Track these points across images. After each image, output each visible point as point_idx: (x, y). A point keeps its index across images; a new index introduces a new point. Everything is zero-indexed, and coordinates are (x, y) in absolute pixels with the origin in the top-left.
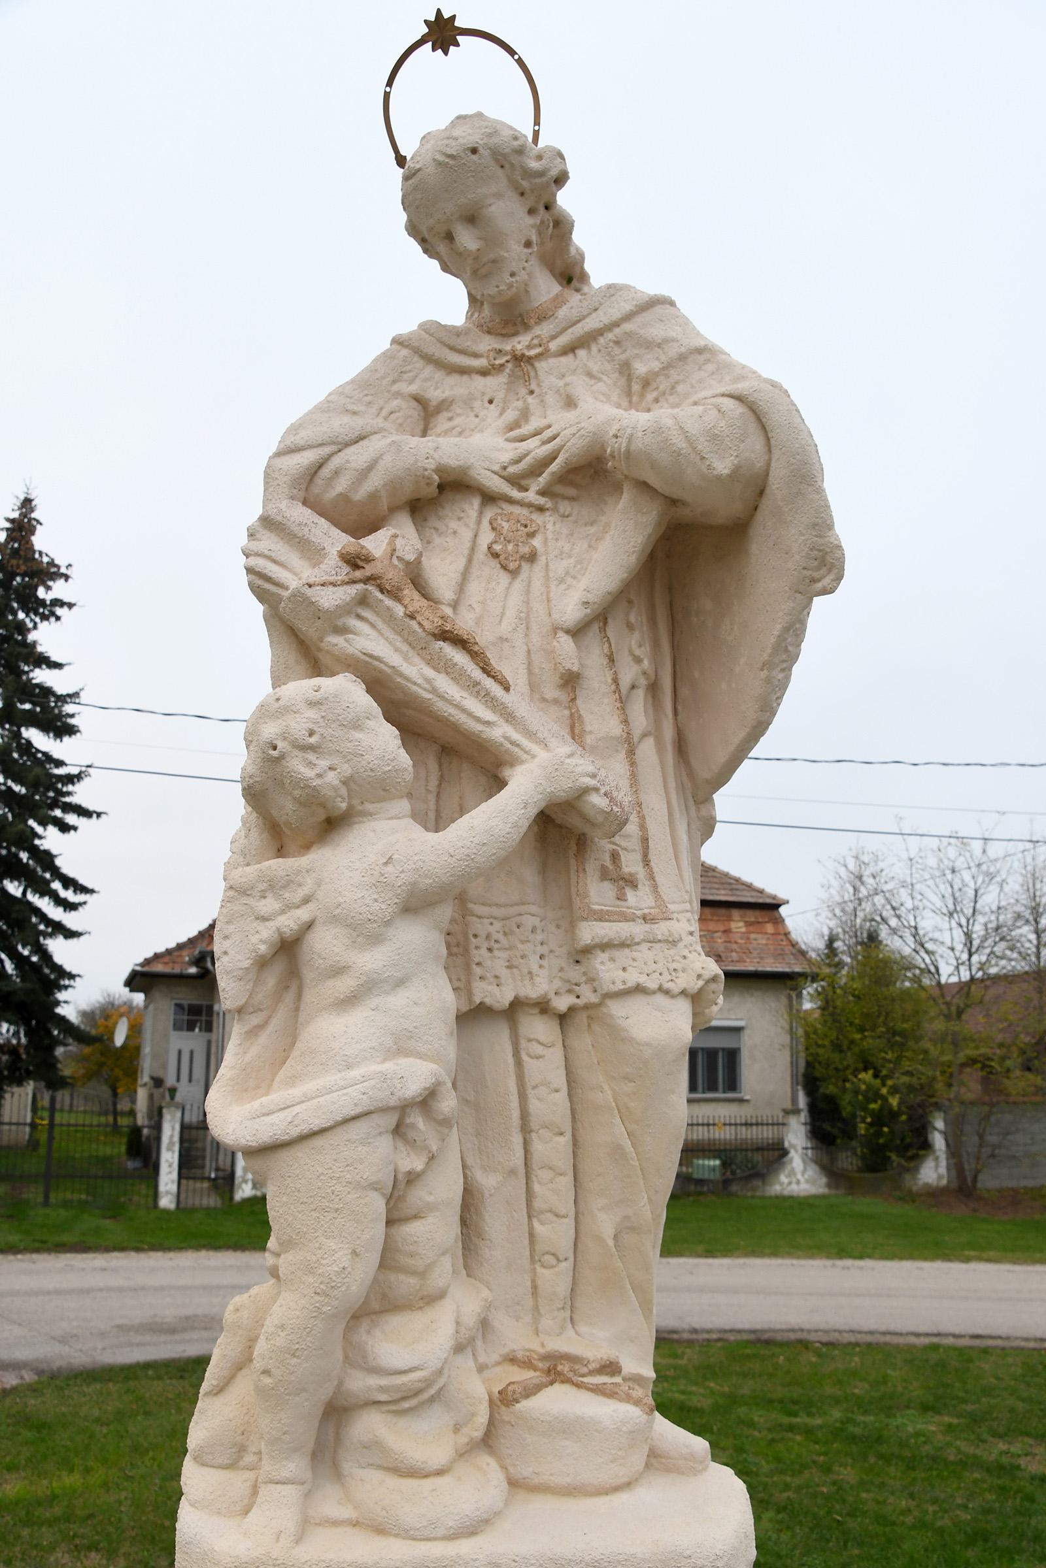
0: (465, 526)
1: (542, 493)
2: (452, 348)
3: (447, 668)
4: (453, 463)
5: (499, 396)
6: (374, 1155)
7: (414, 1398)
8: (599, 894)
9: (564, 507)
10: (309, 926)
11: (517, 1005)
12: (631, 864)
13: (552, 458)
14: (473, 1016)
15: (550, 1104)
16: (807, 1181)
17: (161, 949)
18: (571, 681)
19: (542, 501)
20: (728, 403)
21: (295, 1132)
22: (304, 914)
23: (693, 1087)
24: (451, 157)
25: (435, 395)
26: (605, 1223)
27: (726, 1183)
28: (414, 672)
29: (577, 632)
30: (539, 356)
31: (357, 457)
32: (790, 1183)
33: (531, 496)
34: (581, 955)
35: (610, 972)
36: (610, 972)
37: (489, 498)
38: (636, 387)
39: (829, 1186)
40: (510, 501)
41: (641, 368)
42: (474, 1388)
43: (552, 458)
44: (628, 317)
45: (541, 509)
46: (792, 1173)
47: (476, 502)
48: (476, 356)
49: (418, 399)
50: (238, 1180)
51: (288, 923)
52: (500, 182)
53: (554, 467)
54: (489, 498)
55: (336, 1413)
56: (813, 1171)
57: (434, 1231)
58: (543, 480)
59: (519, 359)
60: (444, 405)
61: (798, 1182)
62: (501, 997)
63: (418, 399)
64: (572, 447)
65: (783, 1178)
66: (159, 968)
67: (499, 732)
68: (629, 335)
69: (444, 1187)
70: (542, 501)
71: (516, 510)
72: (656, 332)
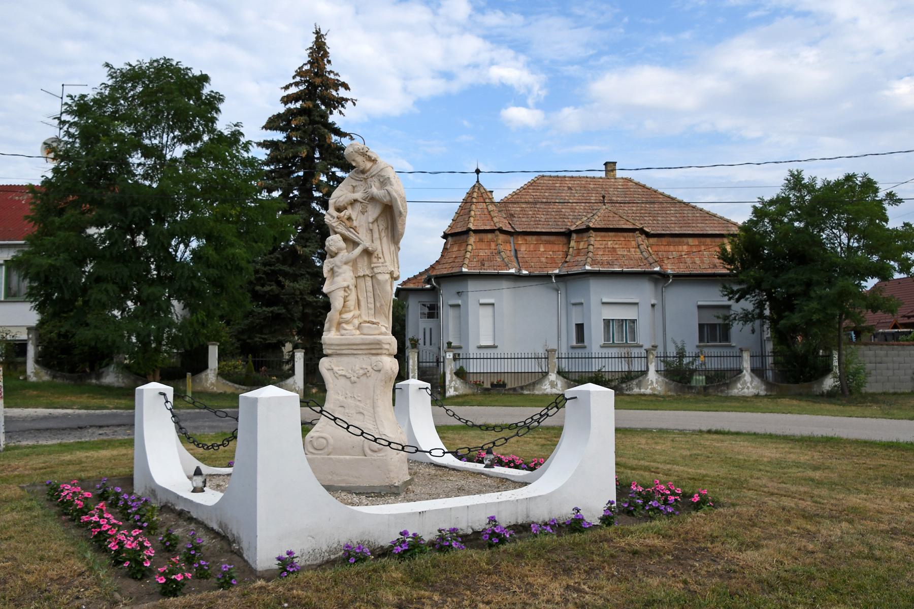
0: (358, 207)
6: (342, 293)
7: (347, 322)
8: (375, 260)
11: (364, 276)
12: (380, 255)
14: (357, 278)
15: (370, 289)
16: (753, 388)
17: (411, 276)
18: (371, 230)
23: (701, 339)
26: (378, 305)
27: (705, 388)
28: (347, 233)
29: (372, 223)
31: (341, 199)
32: (743, 389)
34: (373, 268)
35: (376, 270)
36: (376, 270)
39: (766, 390)
42: (356, 322)
46: (745, 383)
50: (447, 387)
52: (356, 155)
55: (339, 324)
56: (757, 381)
57: (352, 302)
61: (748, 388)
62: (362, 274)
65: (739, 386)
66: (411, 286)
67: (357, 240)
69: (352, 298)
72: (383, 174)
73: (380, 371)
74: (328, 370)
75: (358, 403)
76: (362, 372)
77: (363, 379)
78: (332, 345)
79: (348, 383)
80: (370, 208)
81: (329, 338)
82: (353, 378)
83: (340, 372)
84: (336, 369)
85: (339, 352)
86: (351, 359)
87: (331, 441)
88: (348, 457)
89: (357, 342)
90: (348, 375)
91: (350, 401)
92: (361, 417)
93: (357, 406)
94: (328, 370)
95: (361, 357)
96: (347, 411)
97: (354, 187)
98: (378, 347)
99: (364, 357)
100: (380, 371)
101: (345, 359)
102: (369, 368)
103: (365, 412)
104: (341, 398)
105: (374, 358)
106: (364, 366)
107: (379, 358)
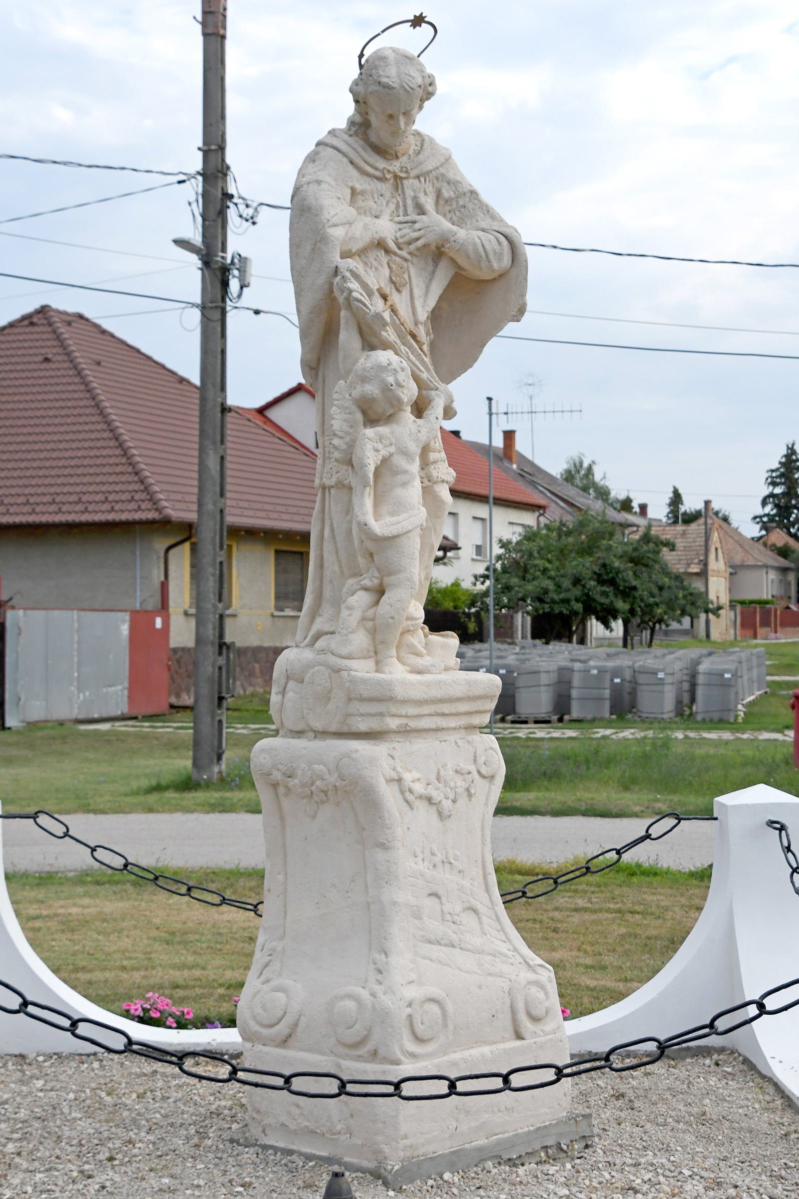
1: (410, 253)
2: (365, 162)
3: (410, 347)
4: (383, 236)
5: (388, 194)
9: (415, 260)
10: (391, 455)
13: (417, 239)
19: (408, 257)
20: (502, 239)
21: (404, 531)
22: (392, 449)
24: (412, 89)
25: (358, 187)
30: (407, 178)
33: (404, 253)
37: (387, 251)
38: (442, 202)
40: (395, 254)
41: (447, 193)
43: (417, 239)
44: (442, 165)
45: (406, 260)
47: (383, 252)
48: (376, 169)
49: (353, 190)
51: (384, 452)
53: (419, 243)
54: (387, 251)
58: (412, 247)
59: (396, 177)
60: (363, 193)
63: (353, 190)
64: (431, 238)
68: (443, 175)
70: (408, 257)
71: (398, 259)
74: (389, 781)
78: (404, 702)
80: (416, 276)
94: (389, 781)
97: (354, 192)
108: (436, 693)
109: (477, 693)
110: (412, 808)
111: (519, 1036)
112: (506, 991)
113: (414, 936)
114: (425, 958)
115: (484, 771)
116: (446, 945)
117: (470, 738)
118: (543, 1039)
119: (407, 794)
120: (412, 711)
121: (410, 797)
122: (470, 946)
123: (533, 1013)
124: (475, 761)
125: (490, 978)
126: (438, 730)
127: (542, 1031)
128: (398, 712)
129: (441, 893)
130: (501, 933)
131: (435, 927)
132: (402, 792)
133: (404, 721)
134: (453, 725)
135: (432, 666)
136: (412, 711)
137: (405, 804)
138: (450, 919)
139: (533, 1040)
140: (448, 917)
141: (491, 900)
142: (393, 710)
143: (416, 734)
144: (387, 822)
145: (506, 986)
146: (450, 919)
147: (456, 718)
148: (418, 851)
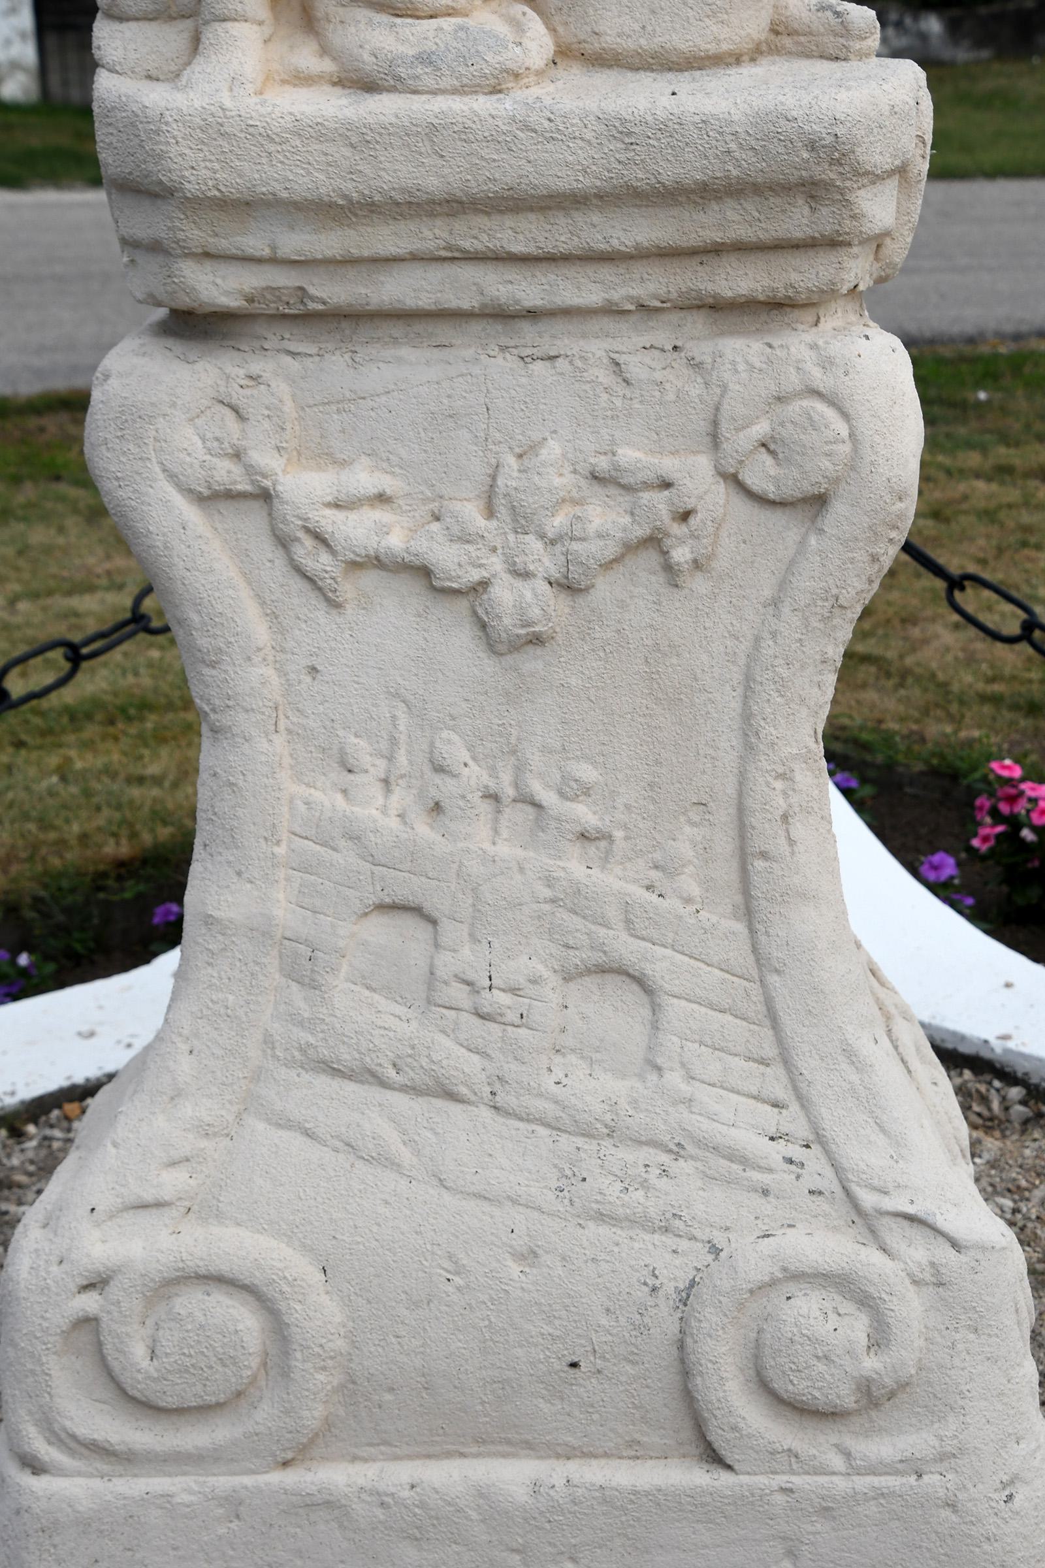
73: (816, 503)
74: (213, 498)
75: (575, 866)
76: (606, 519)
77: (630, 597)
78: (244, 206)
79: (458, 642)
81: (213, 129)
82: (506, 595)
83: (358, 530)
84: (304, 487)
85: (331, 291)
86: (485, 371)
87: (320, 1313)
88: (512, 1476)
89: (559, 170)
90: (446, 557)
91: (490, 846)
92: (613, 1015)
93: (574, 900)
94: (213, 498)
95: (593, 347)
96: (464, 957)
98: (798, 220)
99: (628, 341)
100: (816, 503)
101: (401, 377)
102: (697, 476)
103: (661, 964)
104: (380, 812)
105: (740, 351)
106: (632, 456)
107: (797, 346)
108: (399, 173)
109: (669, 173)
110: (335, 605)
111: (714, 1458)
112: (669, 1288)
113: (268, 1041)
114: (285, 1123)
115: (762, 474)
116: (404, 1089)
117: (702, 350)
118: (841, 1484)
119: (305, 549)
120: (297, 241)
121: (321, 563)
122: (539, 1106)
123: (799, 1387)
124: (715, 439)
125: (594, 1230)
126: (501, 315)
127: (848, 1455)
128: (223, 244)
129: (435, 903)
130: (777, 1071)
131: (379, 1021)
132: (283, 542)
133: (284, 279)
134: (592, 296)
135: (425, 59)
136: (297, 241)
137: (297, 584)
138: (466, 1003)
139: (781, 1480)
140: (458, 994)
141: (755, 950)
142: (195, 234)
143: (397, 329)
144: (203, 642)
145: (674, 1271)
146: (466, 1003)
147: (606, 272)
148: (361, 749)
